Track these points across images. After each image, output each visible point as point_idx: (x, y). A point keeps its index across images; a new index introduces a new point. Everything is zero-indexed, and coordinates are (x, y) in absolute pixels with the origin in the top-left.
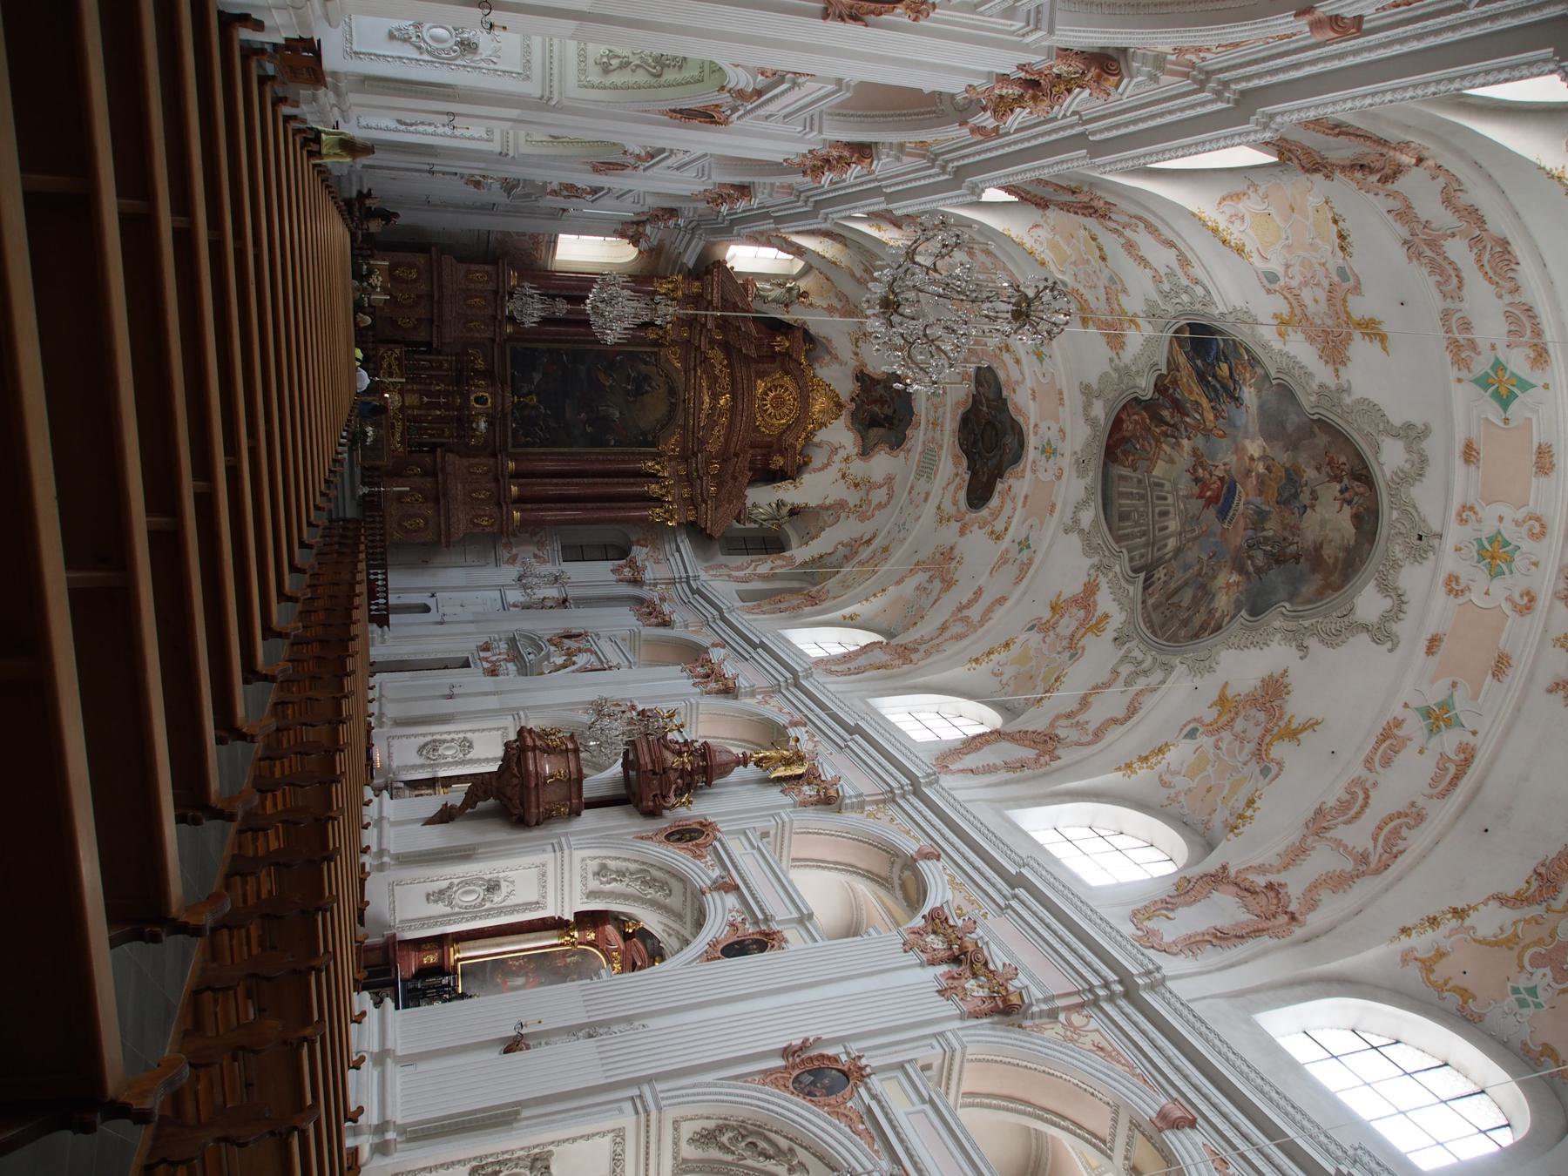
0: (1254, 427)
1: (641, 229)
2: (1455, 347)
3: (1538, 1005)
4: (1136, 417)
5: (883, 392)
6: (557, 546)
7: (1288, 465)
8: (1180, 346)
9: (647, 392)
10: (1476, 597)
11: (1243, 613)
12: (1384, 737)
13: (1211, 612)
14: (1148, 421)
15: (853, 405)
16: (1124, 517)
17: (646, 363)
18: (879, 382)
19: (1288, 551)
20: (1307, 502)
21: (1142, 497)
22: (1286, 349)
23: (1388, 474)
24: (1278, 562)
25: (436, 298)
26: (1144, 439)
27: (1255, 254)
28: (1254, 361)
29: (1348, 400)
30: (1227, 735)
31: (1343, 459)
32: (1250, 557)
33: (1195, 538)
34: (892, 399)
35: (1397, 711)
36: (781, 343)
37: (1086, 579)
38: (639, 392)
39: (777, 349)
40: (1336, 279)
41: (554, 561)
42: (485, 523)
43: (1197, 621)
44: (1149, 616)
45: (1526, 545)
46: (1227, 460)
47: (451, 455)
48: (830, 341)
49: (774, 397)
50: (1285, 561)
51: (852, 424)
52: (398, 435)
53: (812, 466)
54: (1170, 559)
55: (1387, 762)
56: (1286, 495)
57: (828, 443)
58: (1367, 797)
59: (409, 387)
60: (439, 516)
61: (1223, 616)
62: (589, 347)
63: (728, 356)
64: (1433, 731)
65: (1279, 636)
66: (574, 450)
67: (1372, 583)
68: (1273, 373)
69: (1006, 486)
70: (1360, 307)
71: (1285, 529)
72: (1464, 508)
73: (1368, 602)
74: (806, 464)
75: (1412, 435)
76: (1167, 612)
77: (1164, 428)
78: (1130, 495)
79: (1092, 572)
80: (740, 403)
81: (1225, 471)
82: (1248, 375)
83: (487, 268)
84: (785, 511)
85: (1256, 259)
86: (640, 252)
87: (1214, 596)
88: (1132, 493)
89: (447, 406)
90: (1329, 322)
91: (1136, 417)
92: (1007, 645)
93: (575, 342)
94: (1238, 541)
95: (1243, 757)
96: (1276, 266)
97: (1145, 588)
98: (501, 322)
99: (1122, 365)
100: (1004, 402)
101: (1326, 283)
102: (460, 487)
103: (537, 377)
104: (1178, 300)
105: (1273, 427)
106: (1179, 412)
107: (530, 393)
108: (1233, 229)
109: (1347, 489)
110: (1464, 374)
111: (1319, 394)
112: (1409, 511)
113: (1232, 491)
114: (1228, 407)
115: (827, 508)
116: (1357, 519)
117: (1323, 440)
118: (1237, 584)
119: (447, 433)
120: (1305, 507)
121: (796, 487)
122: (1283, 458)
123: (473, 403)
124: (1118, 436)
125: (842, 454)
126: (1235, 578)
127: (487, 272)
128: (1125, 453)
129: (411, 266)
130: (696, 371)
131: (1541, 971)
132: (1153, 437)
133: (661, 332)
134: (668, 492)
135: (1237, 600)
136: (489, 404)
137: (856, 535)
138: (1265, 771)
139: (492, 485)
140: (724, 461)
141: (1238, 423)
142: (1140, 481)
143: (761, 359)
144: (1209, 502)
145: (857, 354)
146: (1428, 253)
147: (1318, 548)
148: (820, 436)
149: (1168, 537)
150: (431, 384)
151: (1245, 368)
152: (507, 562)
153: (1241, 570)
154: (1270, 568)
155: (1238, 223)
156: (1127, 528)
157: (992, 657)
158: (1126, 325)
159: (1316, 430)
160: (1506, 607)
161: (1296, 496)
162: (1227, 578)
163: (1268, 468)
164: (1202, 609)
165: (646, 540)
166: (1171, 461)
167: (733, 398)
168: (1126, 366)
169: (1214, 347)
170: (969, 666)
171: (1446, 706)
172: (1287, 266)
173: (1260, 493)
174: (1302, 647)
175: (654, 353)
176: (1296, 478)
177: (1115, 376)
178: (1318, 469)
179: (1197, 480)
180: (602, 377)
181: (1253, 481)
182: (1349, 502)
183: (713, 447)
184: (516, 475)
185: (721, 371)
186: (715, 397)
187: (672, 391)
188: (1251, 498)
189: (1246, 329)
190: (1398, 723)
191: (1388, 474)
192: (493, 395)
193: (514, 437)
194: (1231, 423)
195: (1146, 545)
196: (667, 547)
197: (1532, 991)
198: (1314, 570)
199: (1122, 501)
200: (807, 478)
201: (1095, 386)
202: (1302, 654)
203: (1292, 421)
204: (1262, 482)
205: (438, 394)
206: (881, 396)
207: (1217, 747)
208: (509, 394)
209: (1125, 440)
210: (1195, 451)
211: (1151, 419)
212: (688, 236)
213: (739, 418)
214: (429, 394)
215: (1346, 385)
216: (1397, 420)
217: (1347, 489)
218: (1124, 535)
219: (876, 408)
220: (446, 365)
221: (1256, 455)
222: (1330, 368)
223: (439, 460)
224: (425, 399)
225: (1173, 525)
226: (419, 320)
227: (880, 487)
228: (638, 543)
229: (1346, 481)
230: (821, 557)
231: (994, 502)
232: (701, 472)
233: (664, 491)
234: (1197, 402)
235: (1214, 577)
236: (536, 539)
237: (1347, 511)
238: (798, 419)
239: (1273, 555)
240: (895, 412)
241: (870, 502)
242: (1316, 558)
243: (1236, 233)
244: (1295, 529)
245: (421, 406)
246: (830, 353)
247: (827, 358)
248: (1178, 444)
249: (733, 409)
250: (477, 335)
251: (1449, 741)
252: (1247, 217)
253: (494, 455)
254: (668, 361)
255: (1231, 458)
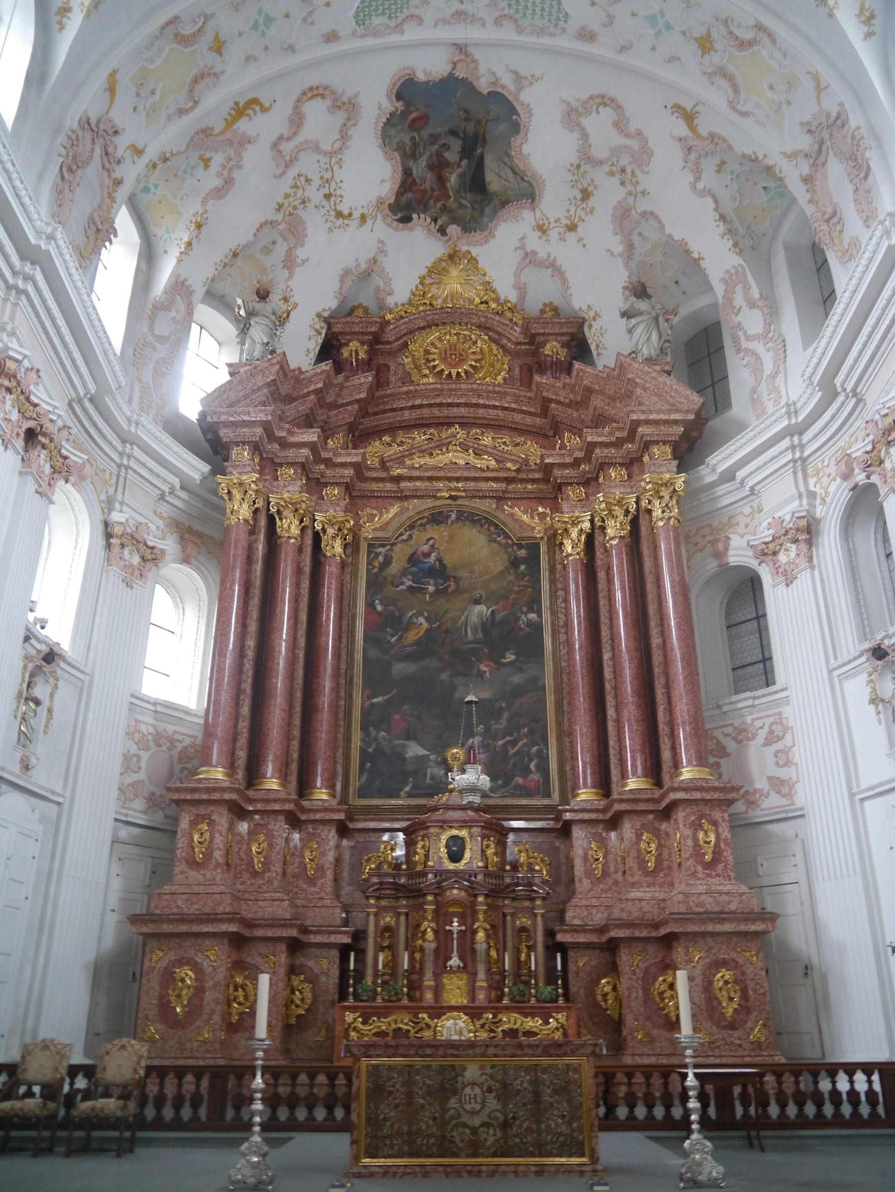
1: (118, 530)
5: (423, 162)
6: (745, 699)
9: (440, 560)
15: (453, 229)
17: (388, 561)
18: (407, 172)
25: (233, 928)
34: (434, 138)
36: (354, 350)
38: (440, 572)
39: (362, 355)
41: (778, 703)
42: (712, 838)
47: (569, 915)
48: (346, 273)
49: (444, 359)
51: (482, 230)
52: (533, 1023)
53: (558, 301)
57: (518, 273)
59: (429, 996)
60: (704, 934)
62: (359, 656)
63: (376, 433)
66: (549, 682)
74: (555, 310)
80: (455, 411)
83: (184, 824)
84: (642, 305)
86: (186, 560)
89: (468, 914)
93: (350, 682)
98: (303, 810)
102: (635, 894)
103: (414, 750)
107: (445, 760)
115: (630, 247)
119: (524, 921)
121: (597, 316)
123: (461, 866)
125: (534, 242)
127: (194, 824)
129: (168, 978)
130: (399, 479)
133: (331, 531)
134: (619, 503)
136: (463, 833)
137: (676, 152)
139: (628, 828)
140: (557, 429)
143: (380, 382)
145: (363, 218)
148: (507, 292)
150: (422, 950)
152: (789, 796)
165: (714, 542)
167: (450, 425)
175: (370, 546)
180: (412, 636)
183: (532, 451)
184: (604, 784)
185: (402, 444)
186: (445, 446)
187: (437, 518)
192: (444, 824)
193: (529, 794)
196: (725, 502)
200: (579, 302)
205: (443, 936)
206: (431, 167)
208: (445, 798)
212: (137, 452)
213: (481, 412)
214: (442, 954)
219: (453, 180)
220: (388, 919)
223: (581, 938)
224: (455, 961)
226: (293, 970)
227: (585, 136)
228: (720, 556)
230: (722, 218)
232: (579, 454)
233: (618, 511)
236: (731, 746)
238: (479, 327)
240: (453, 133)
241: (616, 151)
245: (468, 969)
246: (367, 275)
247: (378, 281)
249: (465, 424)
250: (331, 857)
253: (565, 830)
254: (382, 528)
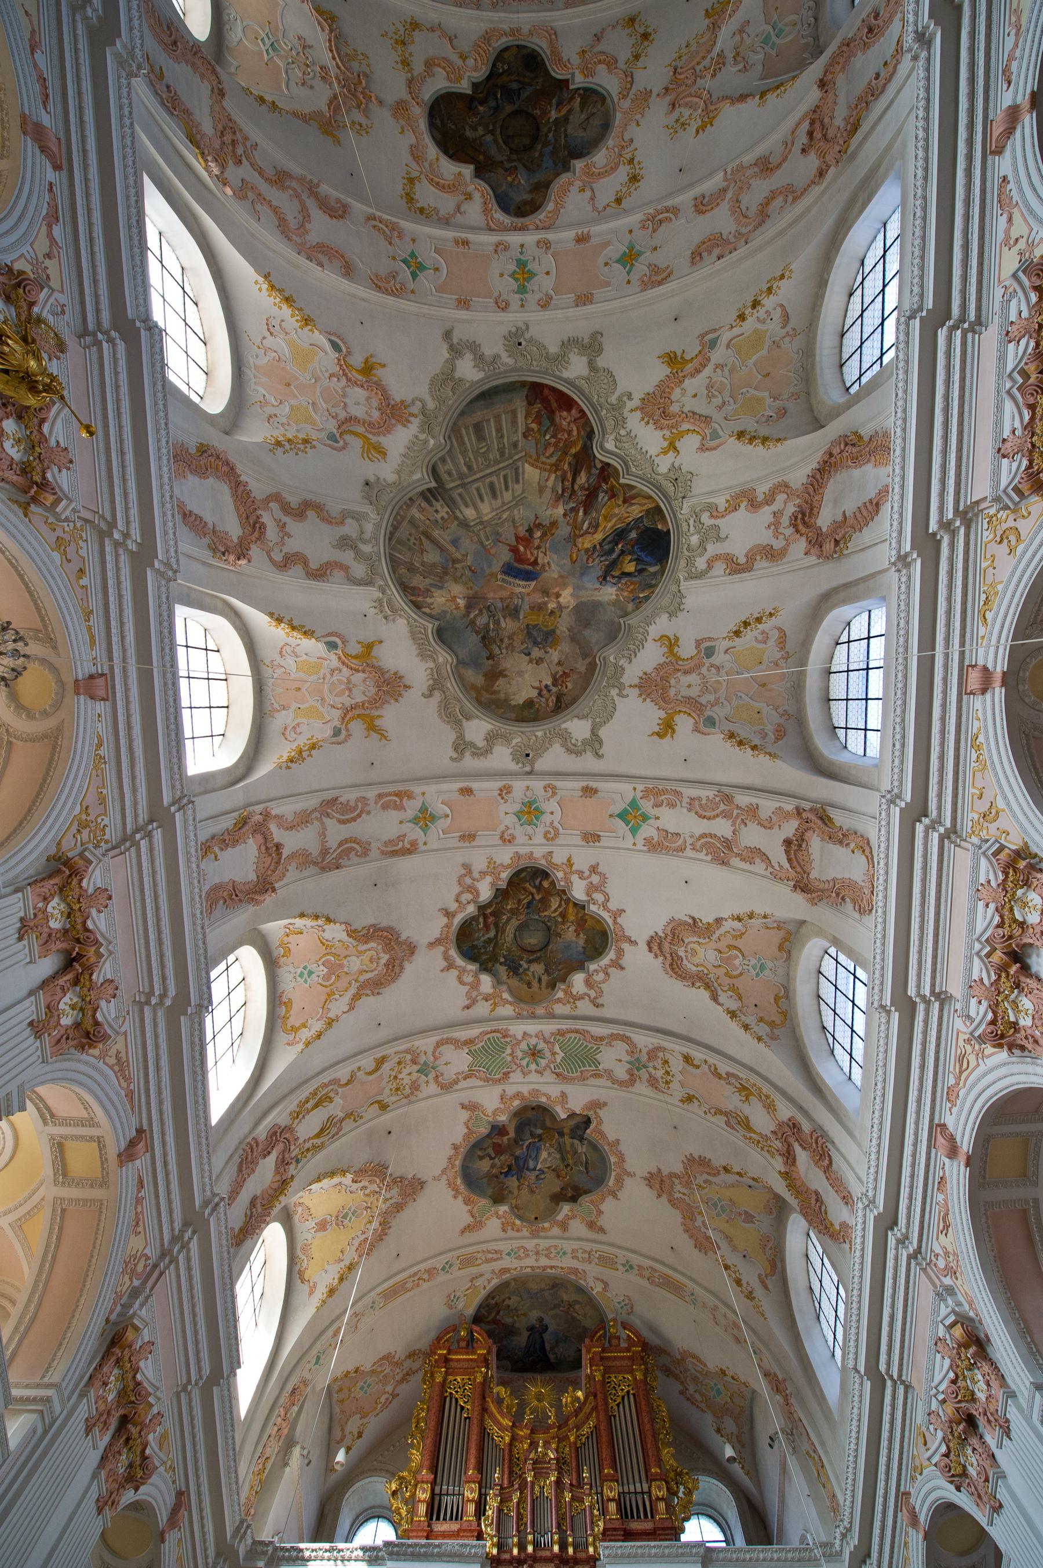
0: (586, 596)
2: (657, 792)
3: (305, 981)
4: (575, 433)
7: (558, 632)
8: (648, 511)
10: (504, 807)
11: (437, 623)
12: (398, 794)
13: (427, 592)
14: (573, 451)
16: (478, 428)
19: (494, 646)
20: (533, 656)
21: (502, 453)
22: (650, 639)
23: (564, 726)
24: (484, 638)
26: (556, 445)
27: (730, 644)
28: (638, 602)
29: (614, 692)
30: (346, 672)
31: (570, 685)
32: (481, 611)
33: (482, 543)
35: (418, 789)
37: (409, 400)
40: (708, 713)
43: (417, 581)
44: (403, 518)
45: (540, 831)
46: (553, 566)
50: (485, 645)
54: (456, 518)
55: (385, 807)
56: (535, 633)
58: (359, 816)
61: (429, 606)
64: (415, 820)
65: (432, 665)
67: (489, 727)
68: (633, 621)
69: (471, 188)
70: (684, 723)
71: (510, 638)
72: (554, 788)
73: (478, 728)
75: (594, 744)
76: (412, 540)
77: (569, 477)
78: (499, 430)
79: (415, 409)
81: (543, 565)
82: (626, 594)
85: (726, 644)
87: (441, 588)
88: (502, 436)
90: (672, 692)
91: (575, 433)
92: (307, 321)
94: (491, 595)
95: (338, 701)
96: (719, 658)
97: (422, 494)
99: (626, 414)
100: (566, 168)
101: (703, 700)
104: (692, 528)
105: (586, 614)
106: (588, 496)
108: (755, 633)
109: (549, 691)
110: (639, 794)
111: (616, 665)
112: (541, 748)
113: (529, 576)
114: (597, 566)
116: (529, 703)
117: (581, 666)
118: (457, 608)
120: (529, 654)
122: (563, 625)
124: (554, 405)
126: (461, 602)
128: (538, 419)
131: (322, 968)
132: (559, 460)
135: (445, 612)
138: (337, 732)
141: (585, 578)
142: (515, 445)
144: (514, 550)
146: (722, 807)
147: (502, 674)
149: (476, 508)
151: (631, 592)
153: (469, 607)
154: (477, 633)
155: (760, 637)
156: (470, 439)
157: (285, 307)
158: (667, 433)
159: (588, 660)
160: (502, 828)
161: (536, 643)
162: (457, 590)
163: (552, 612)
164: (428, 581)
166: (541, 490)
168: (624, 420)
169: (648, 559)
170: (261, 279)
171: (433, 818)
172: (718, 668)
173: (532, 608)
174: (429, 695)
176: (550, 639)
177: (613, 399)
178: (559, 663)
179: (530, 531)
181: (539, 599)
182: (540, 694)
188: (527, 599)
189: (666, 601)
190: (410, 796)
191: (564, 726)
194: (584, 571)
195: (462, 476)
197: (310, 973)
198: (485, 675)
199: (492, 421)
201: (601, 362)
202: (426, 692)
203: (592, 635)
204: (540, 608)
207: (333, 671)
209: (551, 412)
210: (554, 524)
211: (575, 455)
215: (625, 692)
216: (603, 733)
217: (549, 691)
218: (462, 437)
221: (561, 600)
222: (637, 681)
225: (486, 509)
229: (554, 689)
231: (449, 168)
234: (597, 526)
235: (456, 581)
237: (534, 693)
239: (488, 632)
242: (495, 675)
243: (750, 636)
244: (511, 648)
248: (558, 499)
251: (415, 833)
252: (761, 646)
255: (553, 573)
